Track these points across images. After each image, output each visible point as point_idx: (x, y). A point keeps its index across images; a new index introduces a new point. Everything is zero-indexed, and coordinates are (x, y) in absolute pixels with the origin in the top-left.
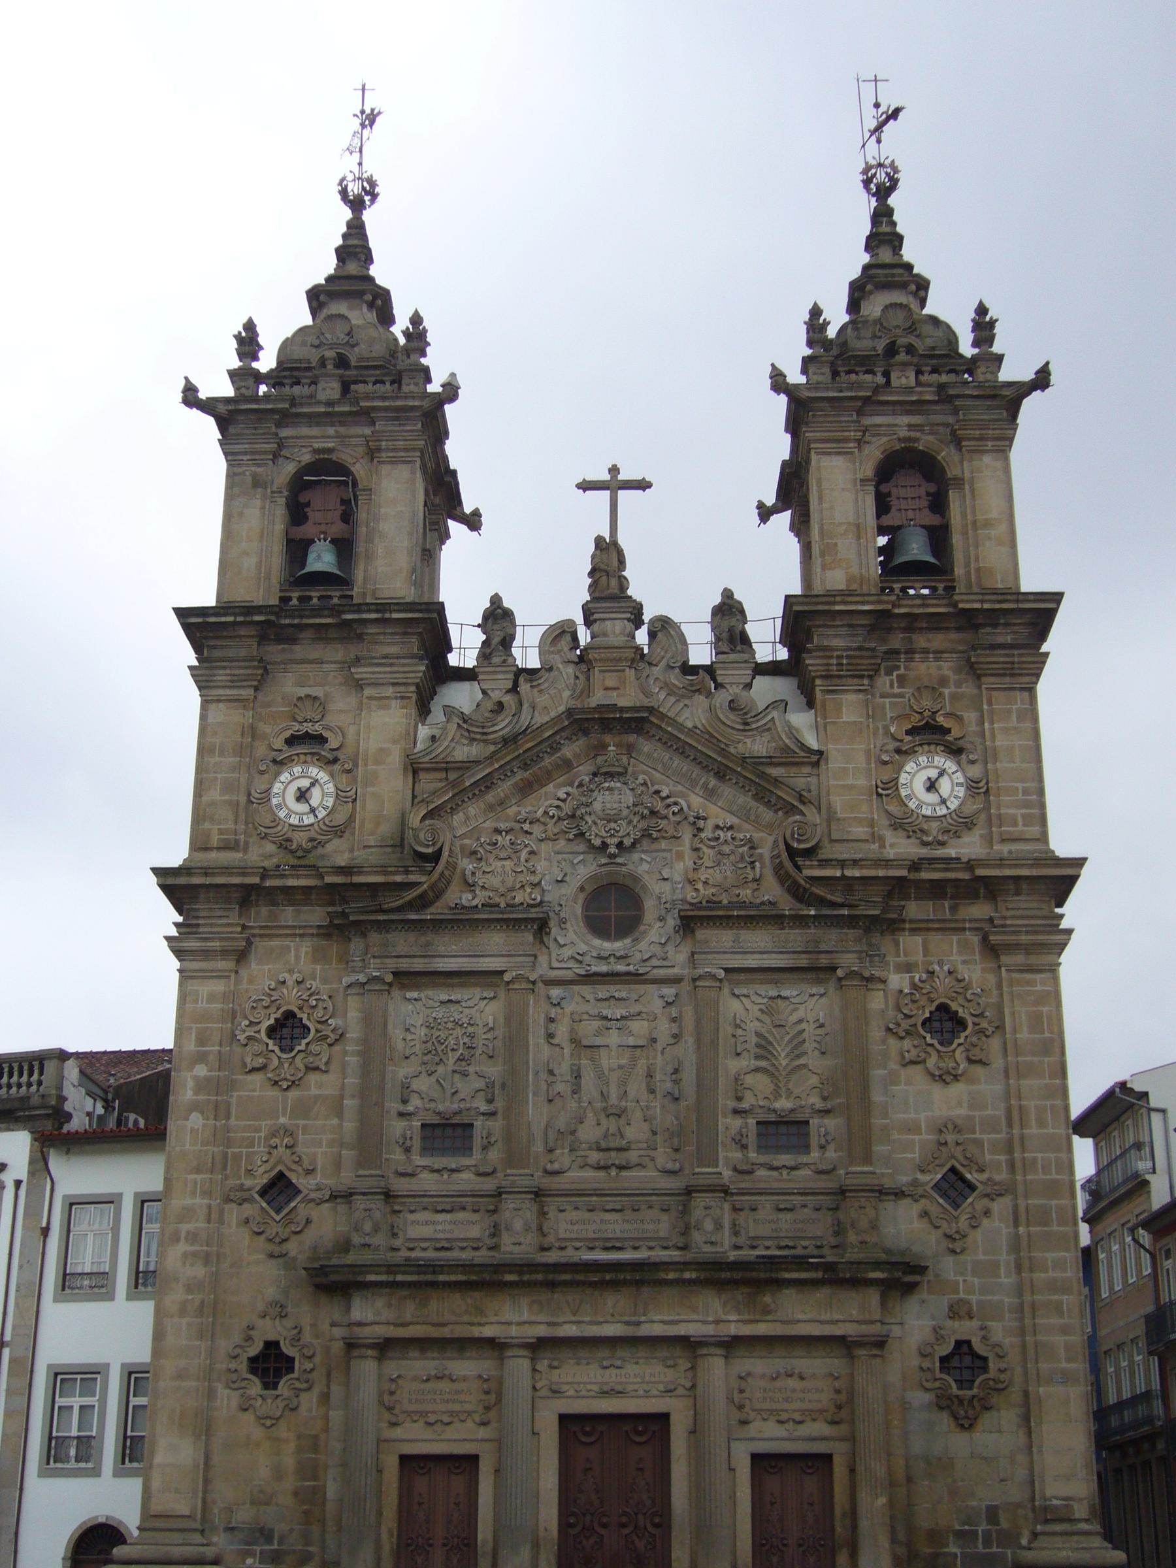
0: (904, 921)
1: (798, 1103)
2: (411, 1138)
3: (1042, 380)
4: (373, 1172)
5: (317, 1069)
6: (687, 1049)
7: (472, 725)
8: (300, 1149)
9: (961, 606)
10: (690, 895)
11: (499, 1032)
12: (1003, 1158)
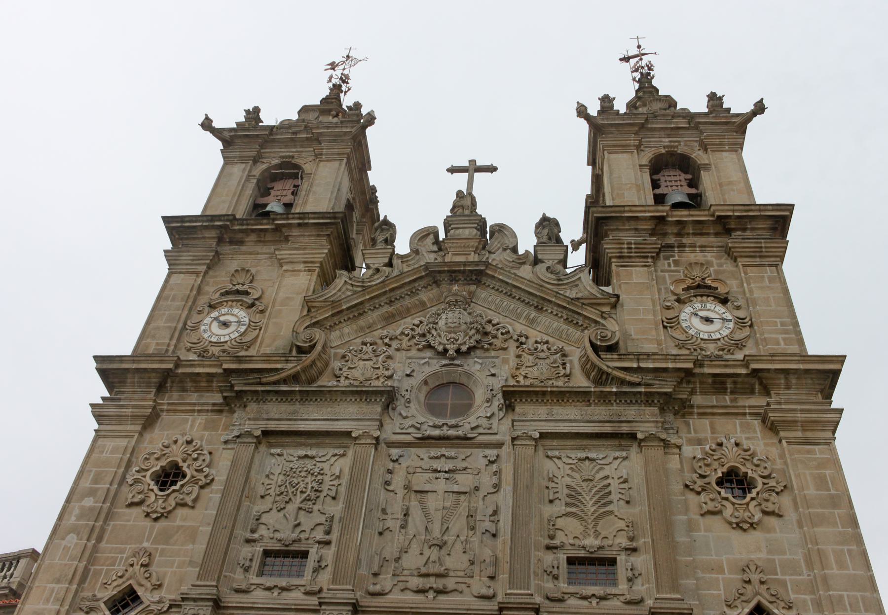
0: (692, 407)
1: (606, 543)
2: (251, 560)
3: (759, 108)
4: (208, 583)
5: (184, 505)
6: (505, 499)
7: (355, 281)
8: (153, 568)
9: (717, 214)
10: (512, 382)
11: (345, 480)
12: (808, 597)
